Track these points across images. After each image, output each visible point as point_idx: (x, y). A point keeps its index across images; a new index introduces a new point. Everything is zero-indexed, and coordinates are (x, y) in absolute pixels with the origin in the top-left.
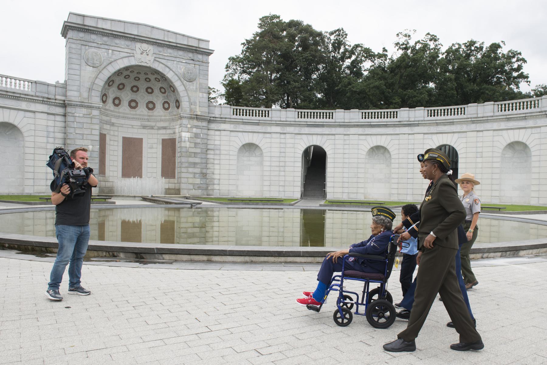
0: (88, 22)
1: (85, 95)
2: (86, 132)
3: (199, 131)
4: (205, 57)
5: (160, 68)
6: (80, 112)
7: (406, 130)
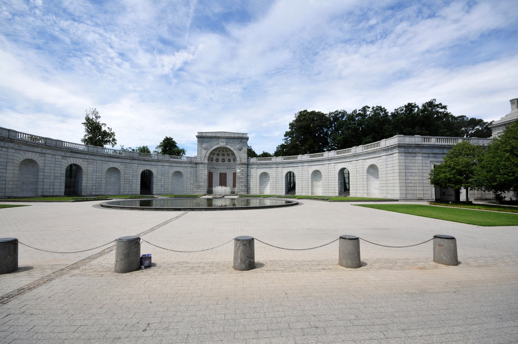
0: (203, 135)
1: (203, 159)
2: (203, 172)
3: (243, 169)
4: (246, 140)
5: (228, 147)
6: (201, 166)
7: (327, 162)
